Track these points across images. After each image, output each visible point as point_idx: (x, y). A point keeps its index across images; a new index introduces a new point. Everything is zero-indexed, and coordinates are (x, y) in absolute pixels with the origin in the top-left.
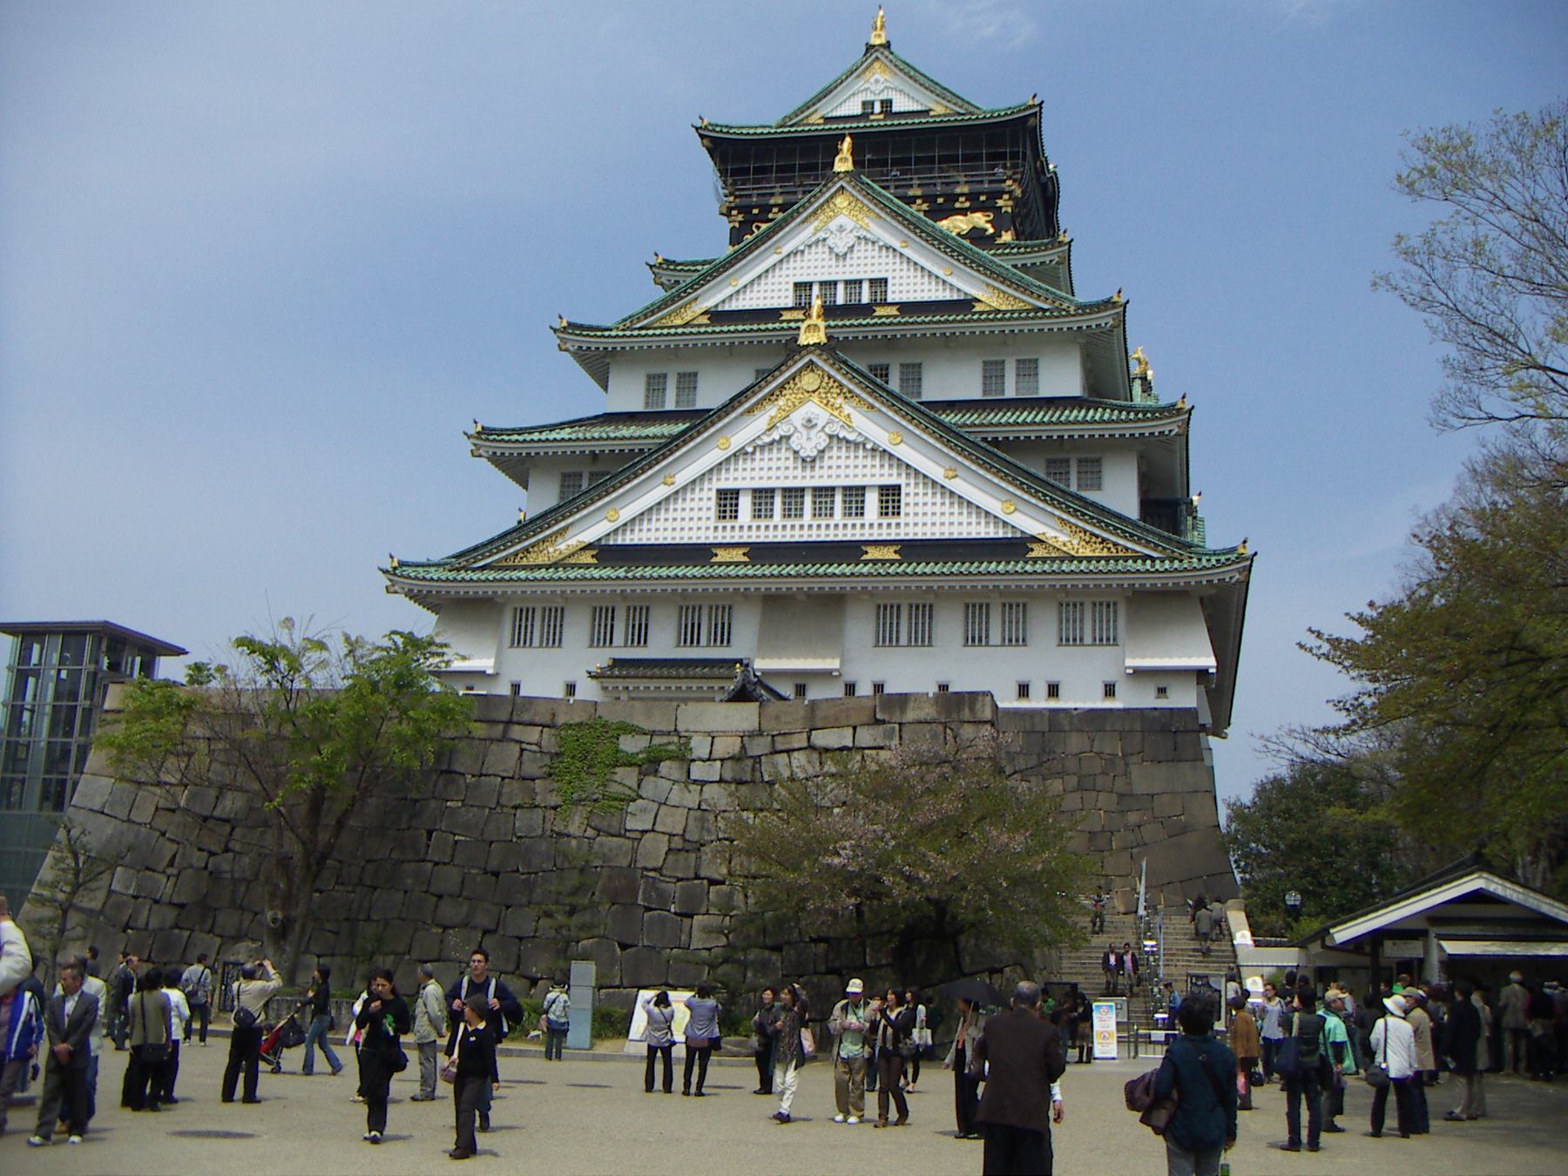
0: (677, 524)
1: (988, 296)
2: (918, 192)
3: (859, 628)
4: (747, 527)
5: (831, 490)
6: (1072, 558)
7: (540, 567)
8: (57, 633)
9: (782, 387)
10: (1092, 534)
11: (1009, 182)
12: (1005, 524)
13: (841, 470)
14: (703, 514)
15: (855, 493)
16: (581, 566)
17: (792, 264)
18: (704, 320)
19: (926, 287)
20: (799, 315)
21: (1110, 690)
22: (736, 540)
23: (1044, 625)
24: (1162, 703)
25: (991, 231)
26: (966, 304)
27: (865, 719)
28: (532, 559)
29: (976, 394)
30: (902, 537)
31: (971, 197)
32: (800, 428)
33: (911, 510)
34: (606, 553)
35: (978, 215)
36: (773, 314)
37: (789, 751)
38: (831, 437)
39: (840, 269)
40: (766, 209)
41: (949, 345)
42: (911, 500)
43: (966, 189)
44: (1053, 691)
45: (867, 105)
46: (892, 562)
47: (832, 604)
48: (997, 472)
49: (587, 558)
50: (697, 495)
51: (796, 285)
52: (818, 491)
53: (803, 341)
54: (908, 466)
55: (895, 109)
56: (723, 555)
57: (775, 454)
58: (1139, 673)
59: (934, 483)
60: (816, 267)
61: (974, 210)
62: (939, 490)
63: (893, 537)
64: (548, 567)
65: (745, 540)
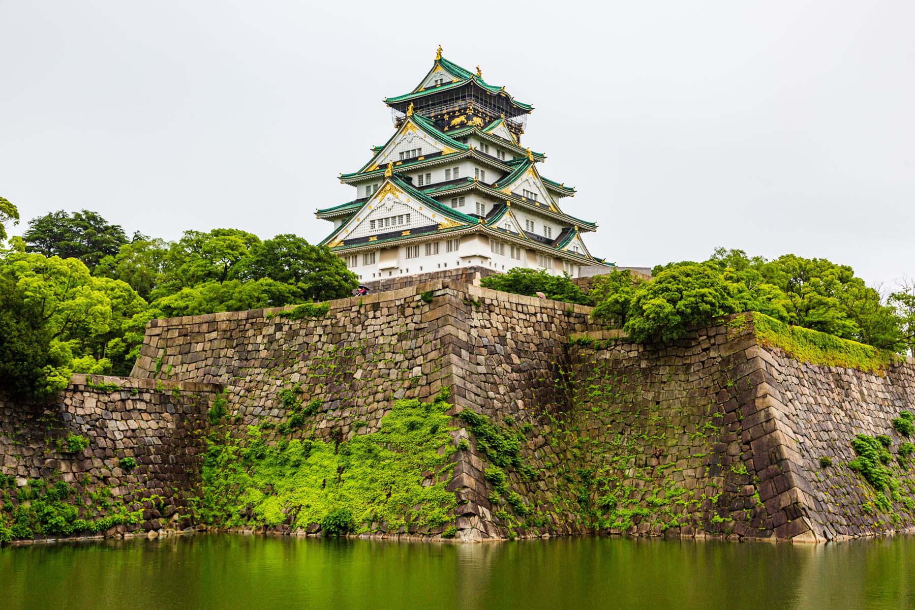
1: (446, 150)
2: (445, 112)
13: (398, 210)
23: (443, 246)
26: (440, 154)
29: (444, 180)
31: (459, 111)
34: (347, 242)
43: (457, 108)
45: (437, 81)
47: (395, 248)
56: (371, 239)
58: (463, 258)
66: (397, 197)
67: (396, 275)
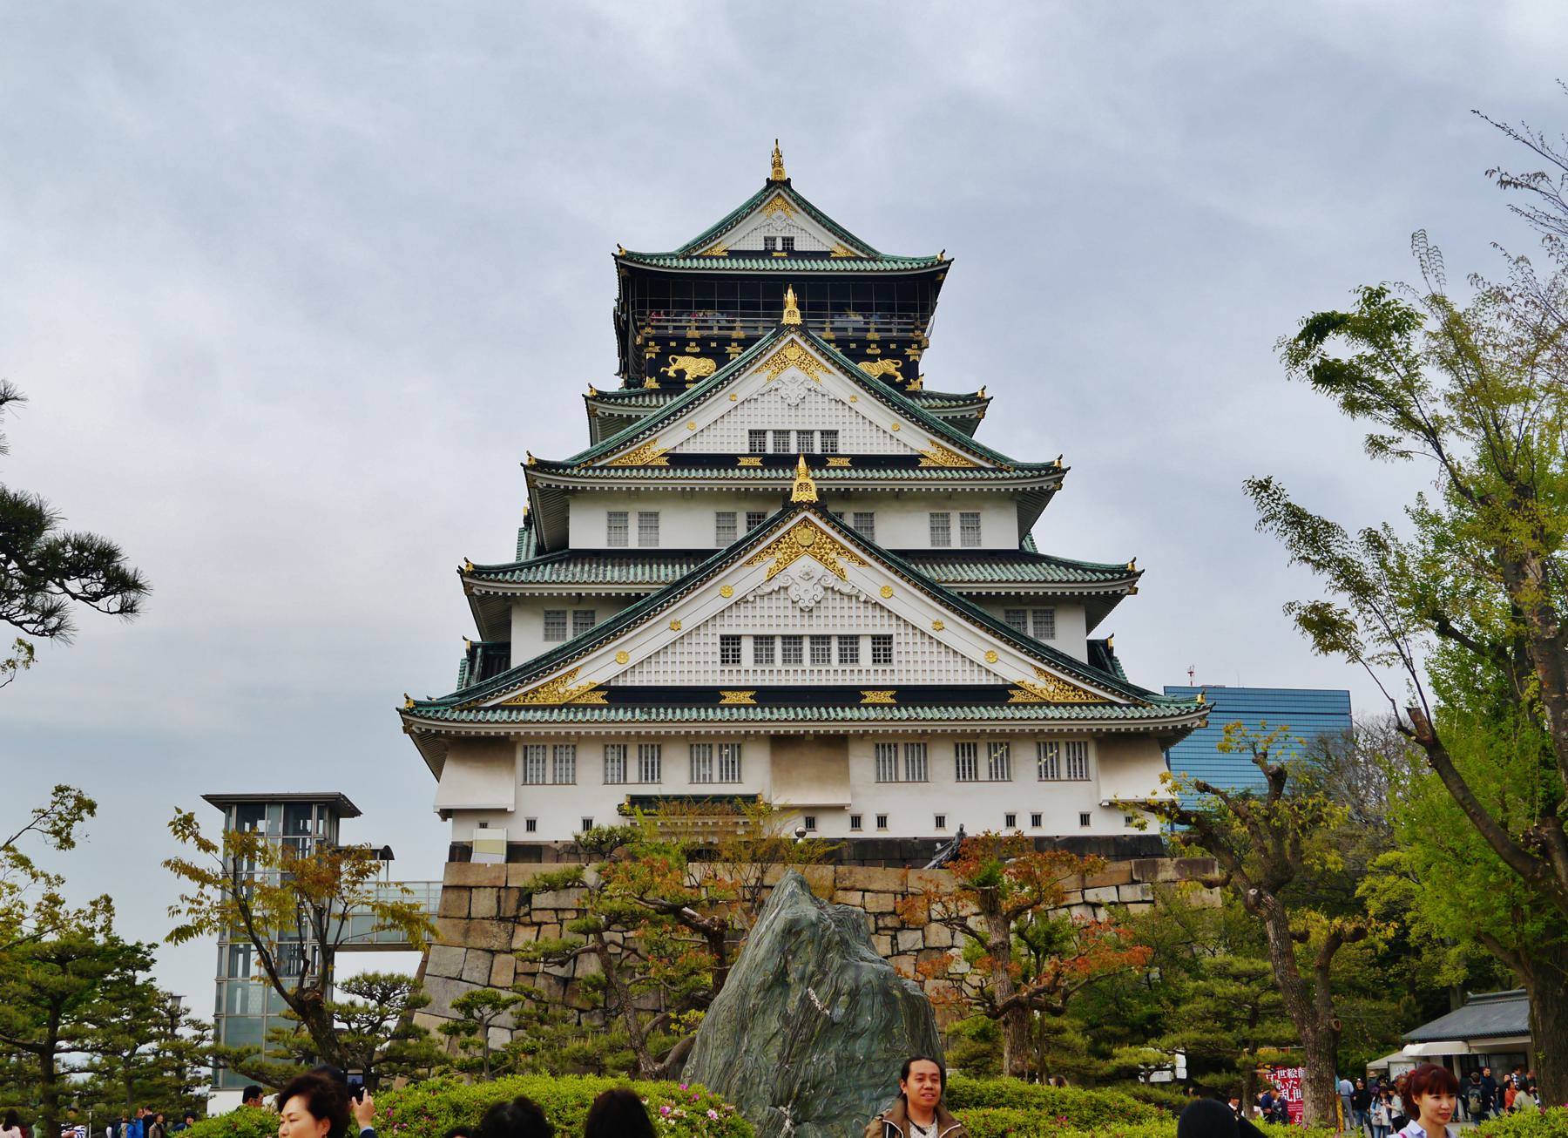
0: (685, 668)
2: (832, 337)
3: (862, 764)
4: (750, 672)
5: (826, 639)
6: (1048, 704)
7: (552, 708)
8: (279, 804)
9: (778, 541)
10: (1065, 683)
11: (918, 333)
12: (988, 671)
13: (834, 622)
14: (710, 658)
15: (849, 642)
16: (593, 707)
17: (746, 412)
18: (664, 462)
19: (875, 440)
20: (756, 462)
21: (1085, 819)
22: (743, 684)
23: (1026, 761)
24: (1135, 832)
25: (900, 378)
26: (910, 462)
27: (1125, 878)
28: (540, 700)
30: (896, 683)
31: (883, 344)
32: (798, 580)
33: (903, 658)
34: (618, 696)
35: (887, 361)
36: (729, 461)
37: (1068, 907)
38: (826, 589)
39: (793, 419)
40: (683, 342)
41: (899, 498)
42: (903, 649)
44: (1036, 820)
46: (890, 706)
47: (837, 743)
48: (981, 626)
49: (597, 698)
50: (702, 639)
51: (751, 432)
52: (815, 639)
53: (795, 498)
54: (898, 618)
55: (798, 246)
56: (731, 698)
57: (774, 603)
58: (1112, 805)
59: (923, 633)
60: (770, 417)
61: (883, 357)
62: (926, 640)
63: (888, 683)
64: (560, 708)
65: (751, 683)
66: (841, 575)
67: (833, 829)
